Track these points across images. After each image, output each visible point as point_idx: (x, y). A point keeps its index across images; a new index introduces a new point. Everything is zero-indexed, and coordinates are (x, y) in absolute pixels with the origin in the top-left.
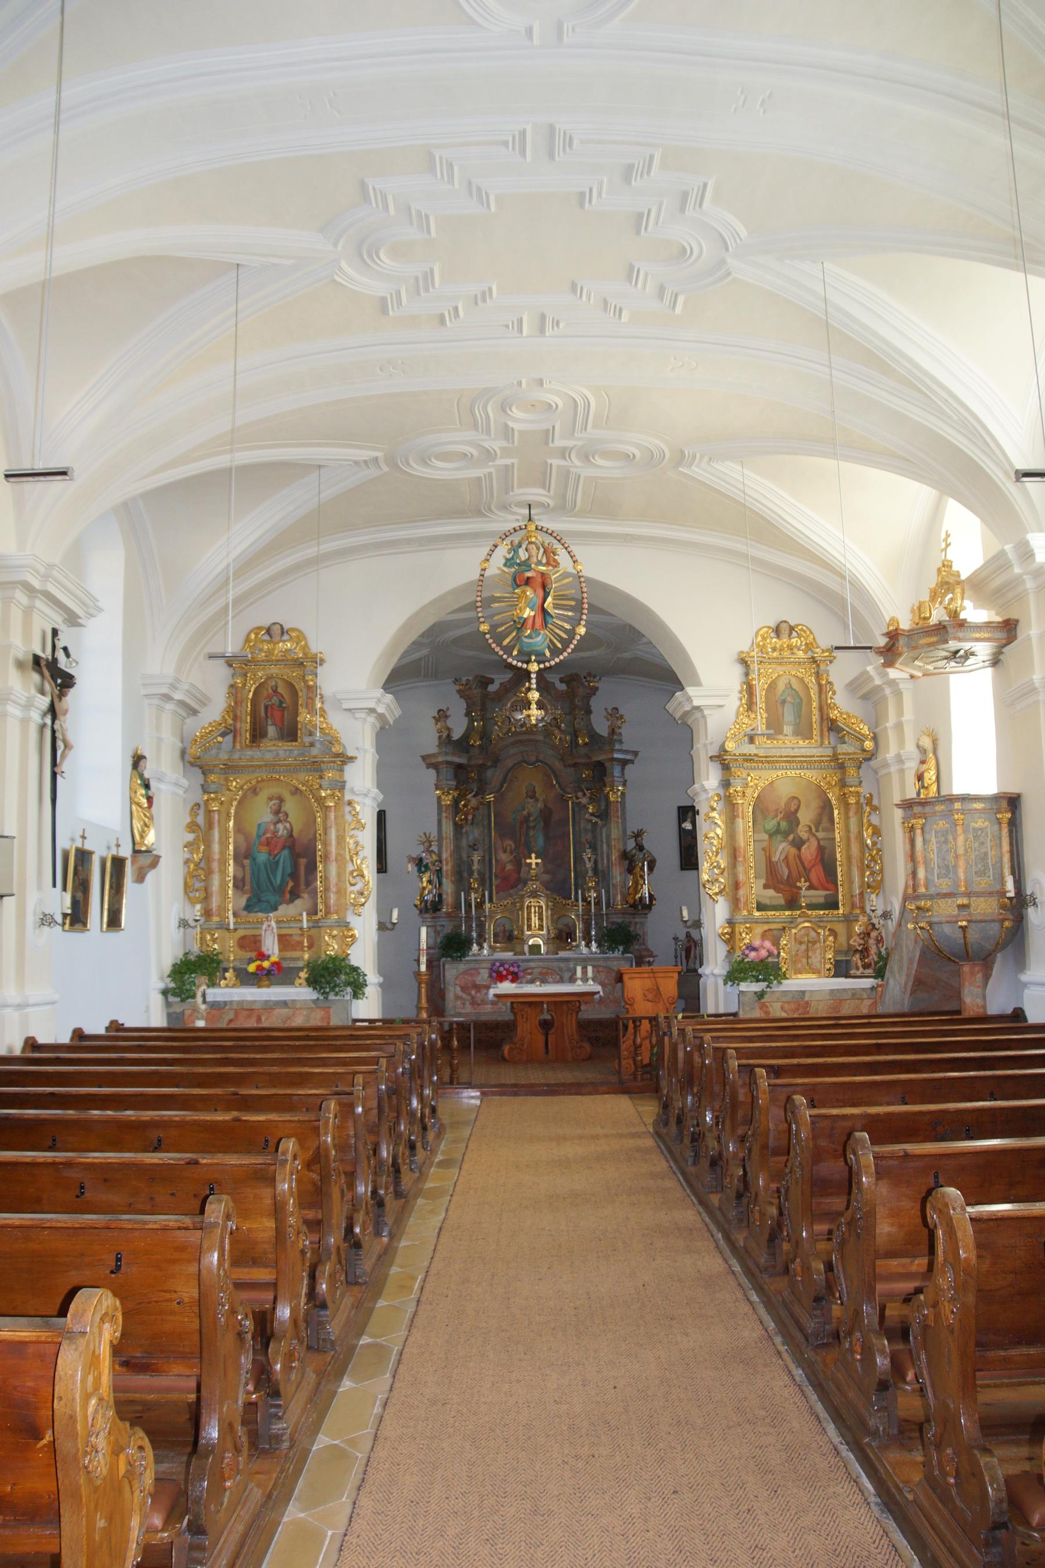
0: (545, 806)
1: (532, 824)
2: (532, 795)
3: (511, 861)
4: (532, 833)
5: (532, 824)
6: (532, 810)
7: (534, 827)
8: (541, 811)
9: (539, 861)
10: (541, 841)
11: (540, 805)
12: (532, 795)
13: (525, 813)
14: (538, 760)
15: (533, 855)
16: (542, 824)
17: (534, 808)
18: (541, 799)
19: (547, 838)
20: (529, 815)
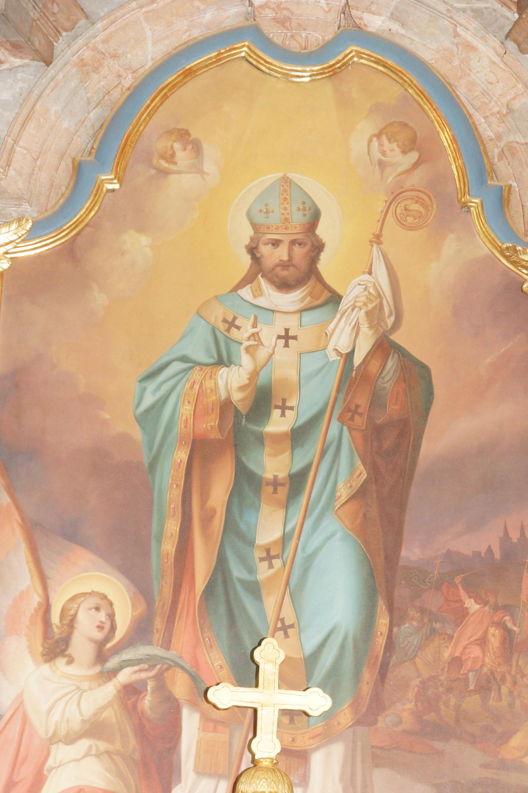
0: (384, 347)
1: (273, 465)
2: (299, 268)
3: (94, 729)
4: (268, 526)
5: (273, 465)
6: (284, 365)
7: (297, 481)
8: (352, 377)
9: (315, 701)
10: (333, 592)
11: (347, 335)
12: (299, 268)
13: (232, 382)
14: (352, 31)
15: (270, 656)
16: (347, 472)
17: (301, 352)
18: (352, 292)
19: (384, 577)
20: (263, 399)
